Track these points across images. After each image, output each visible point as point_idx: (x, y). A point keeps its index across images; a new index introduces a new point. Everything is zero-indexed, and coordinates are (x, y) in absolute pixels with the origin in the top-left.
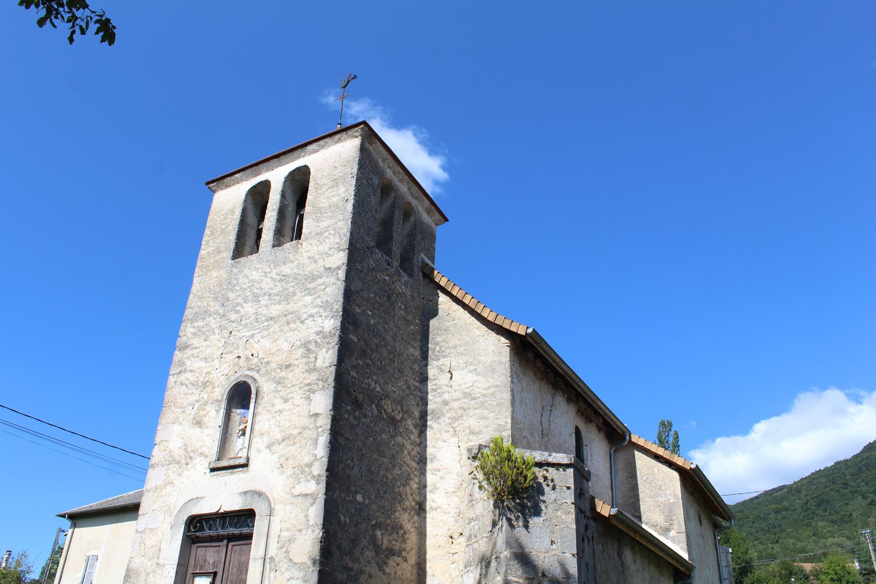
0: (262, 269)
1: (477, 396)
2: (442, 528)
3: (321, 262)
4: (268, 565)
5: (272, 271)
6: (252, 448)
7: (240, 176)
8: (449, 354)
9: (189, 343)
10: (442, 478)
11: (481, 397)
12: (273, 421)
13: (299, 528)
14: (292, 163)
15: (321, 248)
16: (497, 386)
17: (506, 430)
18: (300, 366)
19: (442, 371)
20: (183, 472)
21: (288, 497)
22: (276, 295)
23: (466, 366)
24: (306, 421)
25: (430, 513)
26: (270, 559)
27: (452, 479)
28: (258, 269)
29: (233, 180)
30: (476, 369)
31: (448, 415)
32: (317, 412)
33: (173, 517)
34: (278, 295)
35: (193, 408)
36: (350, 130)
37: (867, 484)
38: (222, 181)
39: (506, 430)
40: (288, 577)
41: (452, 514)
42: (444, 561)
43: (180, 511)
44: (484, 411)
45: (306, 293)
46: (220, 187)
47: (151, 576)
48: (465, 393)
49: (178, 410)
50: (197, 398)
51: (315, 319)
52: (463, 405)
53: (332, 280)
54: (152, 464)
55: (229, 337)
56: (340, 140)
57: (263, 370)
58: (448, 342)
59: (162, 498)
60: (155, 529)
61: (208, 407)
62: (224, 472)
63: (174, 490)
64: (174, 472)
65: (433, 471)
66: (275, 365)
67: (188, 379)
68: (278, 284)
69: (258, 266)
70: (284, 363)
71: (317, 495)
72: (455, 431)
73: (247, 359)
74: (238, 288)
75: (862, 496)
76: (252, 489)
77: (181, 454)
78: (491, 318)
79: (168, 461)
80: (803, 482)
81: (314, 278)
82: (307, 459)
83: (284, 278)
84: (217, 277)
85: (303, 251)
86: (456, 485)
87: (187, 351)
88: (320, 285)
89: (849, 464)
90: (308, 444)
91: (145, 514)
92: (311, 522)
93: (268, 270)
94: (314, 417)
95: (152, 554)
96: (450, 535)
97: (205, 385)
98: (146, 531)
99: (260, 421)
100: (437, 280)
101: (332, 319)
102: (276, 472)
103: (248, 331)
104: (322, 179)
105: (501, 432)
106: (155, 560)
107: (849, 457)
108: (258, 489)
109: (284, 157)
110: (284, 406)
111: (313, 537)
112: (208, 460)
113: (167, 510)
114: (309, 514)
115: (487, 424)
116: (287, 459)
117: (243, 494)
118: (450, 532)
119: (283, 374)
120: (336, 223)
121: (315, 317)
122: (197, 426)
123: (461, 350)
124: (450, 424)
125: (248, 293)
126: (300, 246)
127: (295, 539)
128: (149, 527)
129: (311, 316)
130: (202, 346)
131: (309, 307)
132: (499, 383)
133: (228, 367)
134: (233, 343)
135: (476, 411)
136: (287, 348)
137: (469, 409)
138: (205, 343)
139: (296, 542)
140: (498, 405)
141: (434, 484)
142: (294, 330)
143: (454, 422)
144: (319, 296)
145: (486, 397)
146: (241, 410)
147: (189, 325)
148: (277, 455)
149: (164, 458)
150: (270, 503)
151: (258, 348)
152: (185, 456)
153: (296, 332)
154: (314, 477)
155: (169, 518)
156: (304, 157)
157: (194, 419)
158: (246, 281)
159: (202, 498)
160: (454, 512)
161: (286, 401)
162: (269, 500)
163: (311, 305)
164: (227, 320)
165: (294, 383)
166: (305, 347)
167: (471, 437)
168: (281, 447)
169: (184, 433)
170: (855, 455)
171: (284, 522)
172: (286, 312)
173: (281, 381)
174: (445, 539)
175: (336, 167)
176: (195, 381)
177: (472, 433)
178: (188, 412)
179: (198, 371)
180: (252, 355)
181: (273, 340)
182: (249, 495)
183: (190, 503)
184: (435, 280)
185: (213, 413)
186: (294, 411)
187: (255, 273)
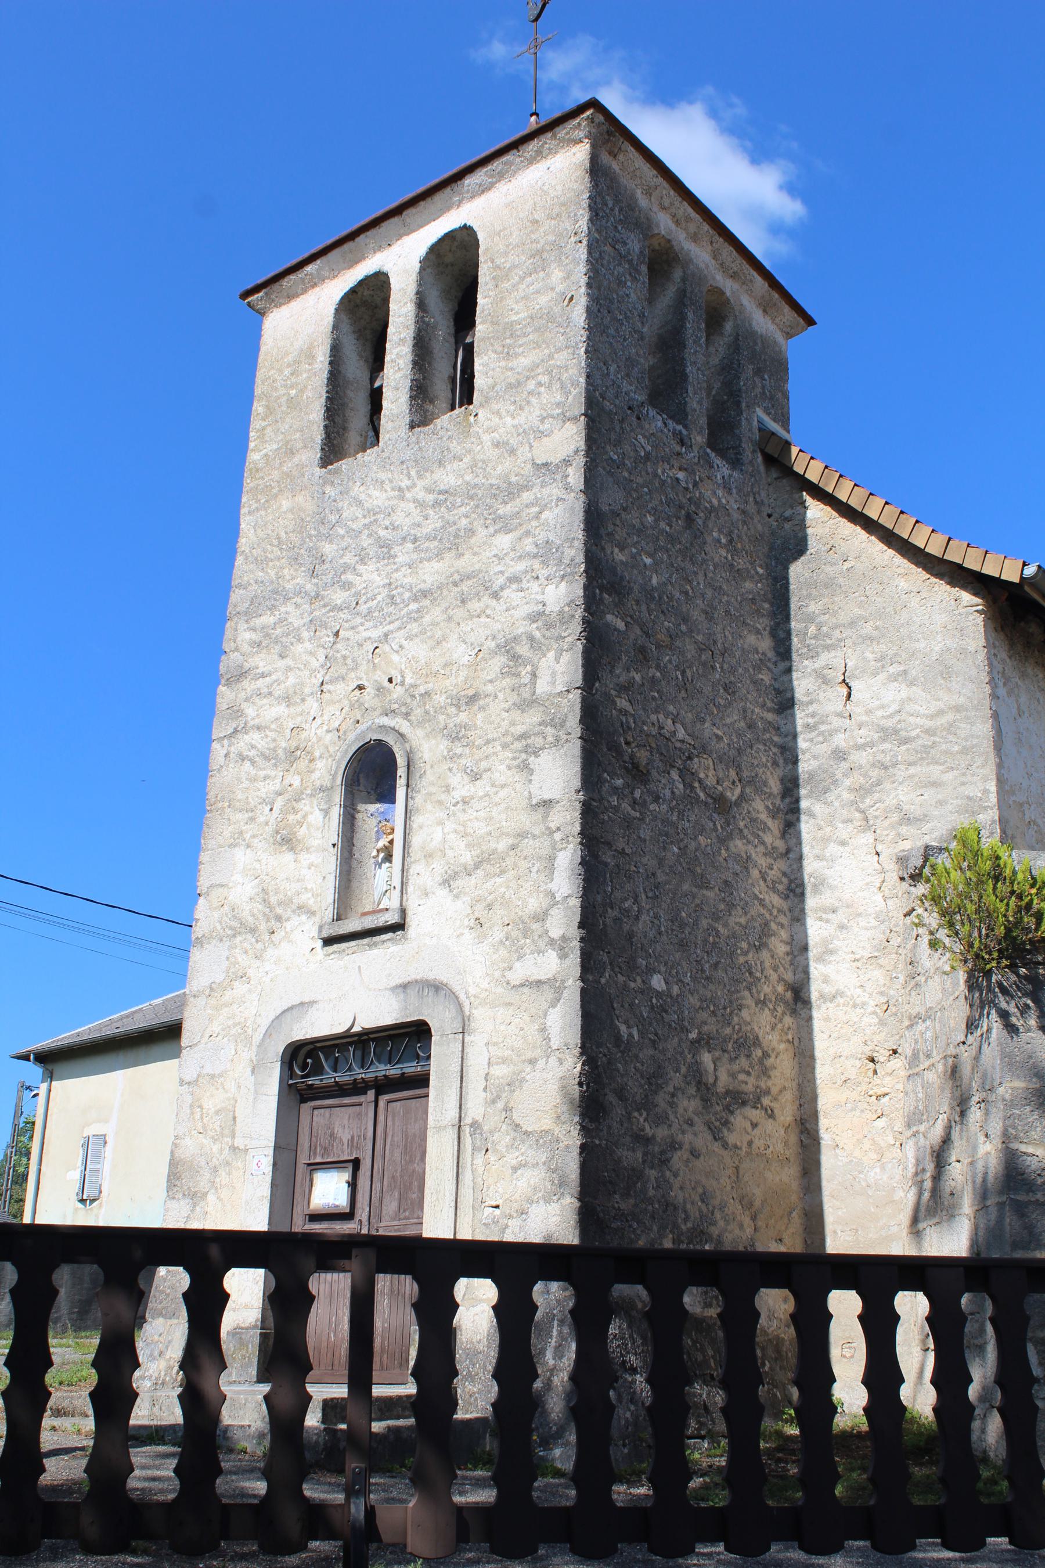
0: (391, 481)
1: (913, 734)
2: (849, 1040)
3: (524, 453)
4: (467, 1141)
5: (414, 485)
6: (410, 889)
8: (840, 640)
9: (247, 666)
10: (842, 927)
11: (922, 735)
12: (450, 826)
13: (529, 1055)
14: (433, 223)
15: (521, 419)
16: (957, 709)
17: (985, 808)
18: (501, 696)
19: (826, 681)
20: (264, 950)
21: (500, 990)
22: (429, 538)
23: (883, 667)
24: (525, 820)
25: (819, 1007)
26: (471, 1126)
27: (866, 929)
28: (383, 482)
29: (303, 280)
30: (905, 672)
31: (847, 782)
32: (546, 797)
33: (254, 1048)
34: (435, 538)
35: (271, 810)
36: (561, 127)
38: (276, 287)
39: (985, 808)
40: (514, 1162)
41: (870, 1009)
42: (857, 1113)
43: (268, 1034)
44: (931, 767)
45: (497, 527)
47: (222, 1173)
48: (882, 730)
49: (239, 816)
50: (278, 787)
51: (525, 585)
52: (880, 757)
53: (555, 491)
54: (197, 938)
55: (334, 643)
56: (539, 156)
57: (418, 712)
58: (835, 614)
59: (226, 1009)
60: (221, 1075)
61: (305, 806)
62: (353, 943)
63: (250, 991)
64: (246, 952)
65: (820, 914)
66: (444, 697)
67: (253, 747)
68: (431, 512)
69: (383, 476)
70: (462, 693)
71: (563, 982)
72: (866, 819)
73: (380, 689)
74: (341, 532)
76: (418, 977)
77: (255, 911)
78: (934, 548)
79: (231, 928)
81: (511, 491)
82: (534, 903)
83: (444, 497)
84: (291, 510)
85: (481, 431)
86: (876, 942)
87: (245, 683)
88: (527, 506)
90: (534, 869)
92: (555, 1043)
93: (405, 483)
94: (541, 810)
95: (218, 1129)
96: (869, 1054)
97: (292, 755)
98: (200, 1080)
99: (421, 827)
100: (799, 468)
101: (563, 584)
102: (468, 936)
103: (376, 626)
104: (506, 254)
105: (974, 813)
106: (226, 1139)
108: (430, 976)
110: (473, 789)
111: (561, 1074)
112: (317, 919)
113: (240, 1034)
114: (549, 1024)
115: (940, 797)
116: (489, 907)
117: (400, 990)
118: (870, 1048)
119: (463, 717)
120: (551, 357)
121: (524, 581)
122: (284, 848)
123: (868, 629)
124: (854, 803)
125: (365, 541)
126: (472, 419)
127: (523, 1080)
128: (205, 1071)
129: (515, 579)
131: (507, 560)
132: (962, 700)
133: (338, 713)
134: (345, 658)
135: (912, 770)
136: (467, 658)
137: (895, 764)
138: (281, 664)
139: (525, 1086)
140: (965, 751)
141: (826, 942)
142: (479, 616)
143: (863, 798)
144: (528, 533)
145: (934, 734)
146: (378, 806)
147: (243, 626)
148: (467, 899)
149: (220, 922)
150: (460, 1006)
151: (401, 663)
152: (265, 914)
153: (483, 619)
154: (552, 942)
155: (246, 1050)
156: (458, 206)
157: (277, 832)
158: (359, 513)
159: (312, 1003)
160: (872, 1003)
162: (457, 998)
163: (512, 555)
164: (325, 606)
165: (490, 736)
166: (508, 652)
167: (904, 830)
168: (473, 880)
169: (257, 866)
171: (495, 1044)
172: (456, 577)
173: (461, 734)
174: (858, 1063)
175: (537, 222)
176: (269, 749)
177: (907, 820)
178: (262, 819)
179: (273, 726)
180: (390, 680)
181: (431, 643)
182: (412, 992)
183: (288, 1015)
184: (795, 468)
185: (316, 817)
186: (497, 799)
187: (376, 493)
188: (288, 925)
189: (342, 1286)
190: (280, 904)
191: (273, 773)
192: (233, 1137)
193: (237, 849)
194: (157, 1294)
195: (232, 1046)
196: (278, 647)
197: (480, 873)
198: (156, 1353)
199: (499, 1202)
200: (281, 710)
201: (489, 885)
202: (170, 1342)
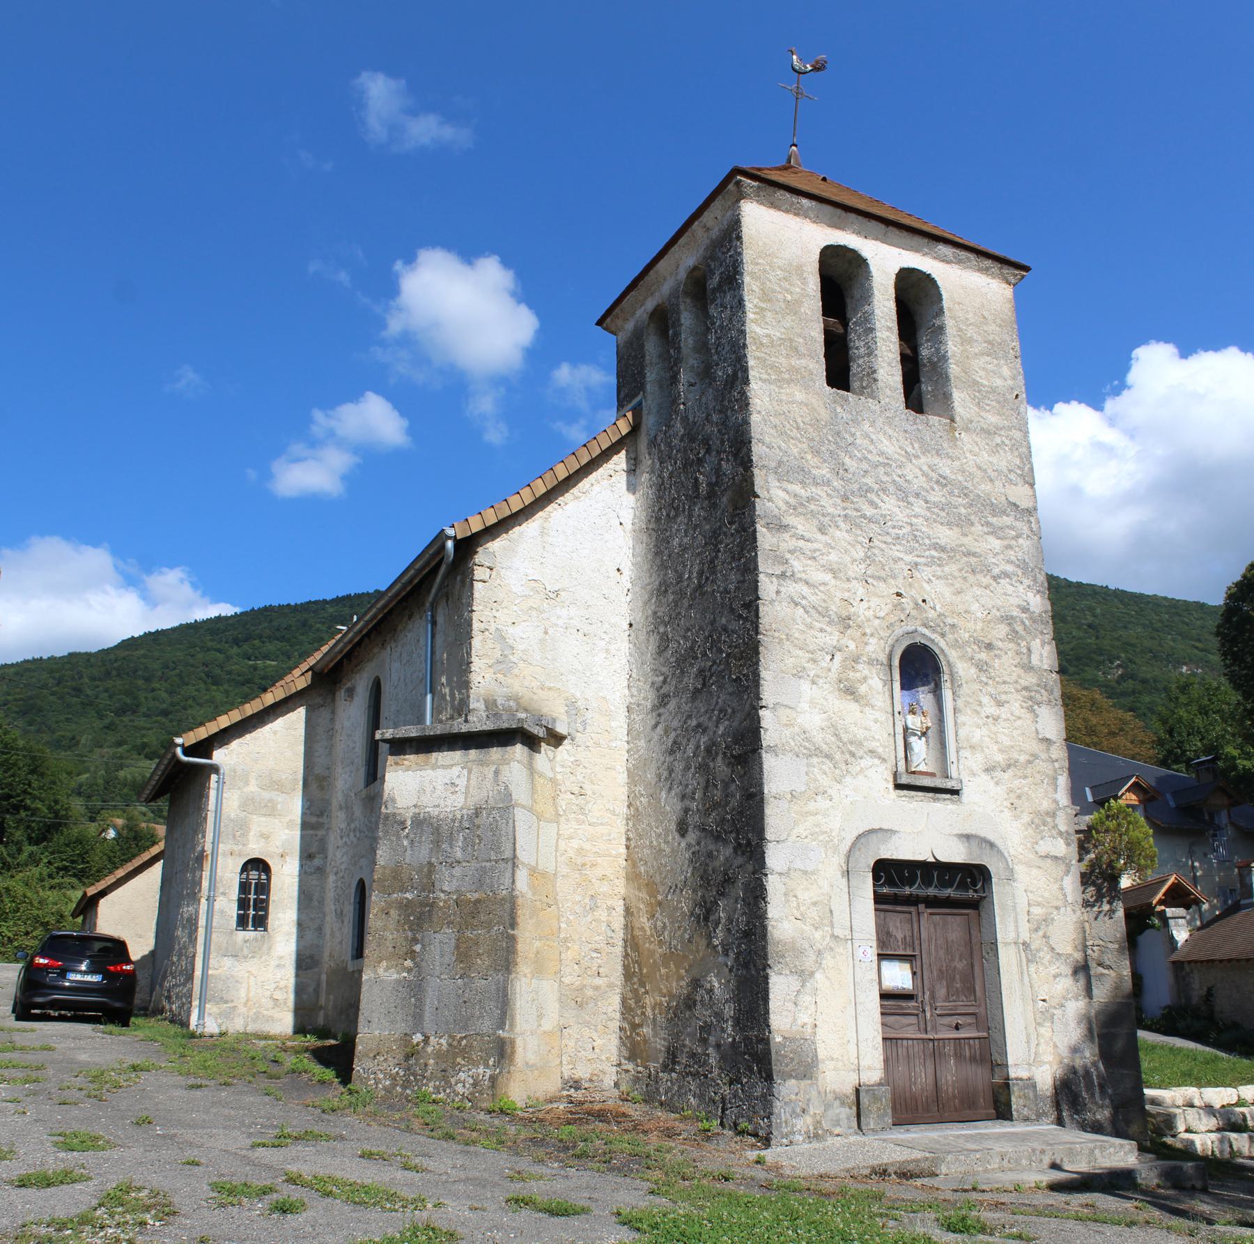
12: (985, 731)
15: (994, 460)
20: (844, 776)
22: (936, 505)
24: (1035, 747)
32: (1048, 736)
34: (943, 509)
37: (111, 697)
46: (759, 196)
47: (827, 955)
49: (800, 653)
56: (985, 271)
57: (950, 637)
60: (813, 873)
62: (920, 794)
64: (825, 773)
66: (967, 635)
67: (804, 598)
71: (1071, 861)
75: (97, 712)
80: (7, 670)
82: (1046, 805)
87: (786, 536)
89: (92, 660)
92: (1070, 899)
99: (964, 724)
102: (1007, 814)
107: (94, 650)
109: (894, 229)
111: (1075, 920)
117: (964, 839)
122: (849, 697)
130: (816, 541)
154: (1060, 834)
159: (893, 832)
161: (1000, 704)
164: (856, 510)
165: (1005, 679)
168: (1006, 776)
169: (825, 703)
170: (103, 650)
180: (924, 601)
182: (974, 843)
183: (874, 837)
188: (863, 763)
189: (916, 1050)
190: (851, 743)
193: (802, 681)
194: (780, 1058)
195: (823, 850)
197: (1010, 772)
198: (798, 1110)
199: (1047, 997)
200: (828, 577)
201: (1017, 782)
202: (809, 1100)
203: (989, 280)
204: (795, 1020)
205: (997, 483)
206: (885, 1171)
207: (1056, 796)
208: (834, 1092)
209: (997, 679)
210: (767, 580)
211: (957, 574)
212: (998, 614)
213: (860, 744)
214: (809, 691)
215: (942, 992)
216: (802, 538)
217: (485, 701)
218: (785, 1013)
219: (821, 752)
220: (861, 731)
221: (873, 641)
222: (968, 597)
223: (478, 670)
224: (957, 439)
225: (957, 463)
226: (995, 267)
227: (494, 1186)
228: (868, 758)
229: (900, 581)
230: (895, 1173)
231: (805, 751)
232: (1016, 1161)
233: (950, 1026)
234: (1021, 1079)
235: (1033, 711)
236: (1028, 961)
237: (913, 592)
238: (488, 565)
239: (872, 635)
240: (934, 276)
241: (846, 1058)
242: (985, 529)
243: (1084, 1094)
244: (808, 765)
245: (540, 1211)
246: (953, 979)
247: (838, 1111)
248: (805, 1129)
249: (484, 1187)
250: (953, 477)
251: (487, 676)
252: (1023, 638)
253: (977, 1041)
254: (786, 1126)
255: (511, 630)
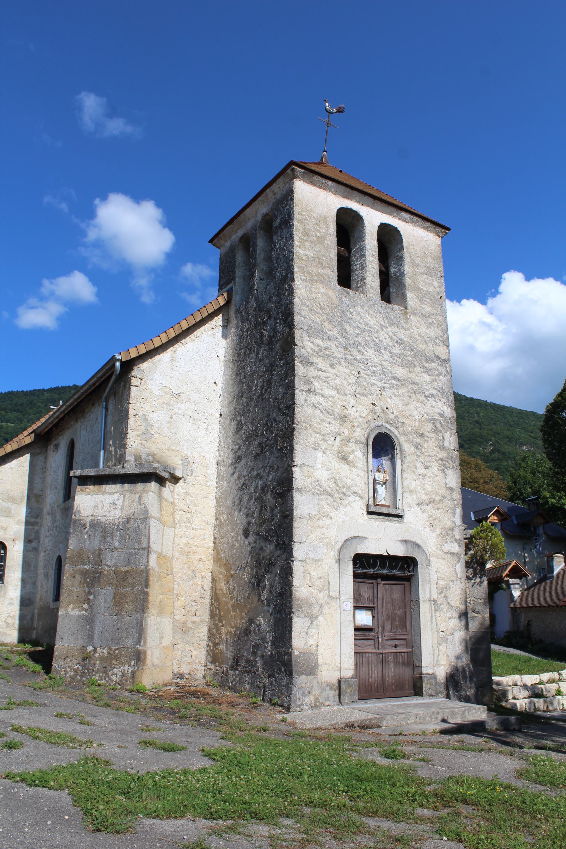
7: (331, 186)
12: (418, 483)
13: (451, 578)
20: (339, 506)
21: (440, 552)
24: (445, 492)
29: (323, 183)
32: (451, 486)
34: (399, 358)
38: (311, 174)
46: (304, 178)
49: (317, 435)
56: (426, 228)
57: (401, 429)
61: (352, 446)
62: (381, 517)
64: (329, 504)
66: (410, 428)
67: (321, 404)
79: (318, 490)
82: (449, 524)
87: (312, 368)
91: (303, 542)
92: (459, 576)
99: (407, 479)
102: (428, 529)
108: (414, 540)
109: (378, 202)
117: (404, 543)
122: (344, 462)
127: (450, 587)
130: (328, 372)
154: (456, 540)
159: (365, 538)
161: (426, 468)
164: (351, 355)
168: (428, 508)
169: (330, 465)
171: (439, 572)
180: (387, 408)
183: (354, 541)
188: (350, 499)
189: (373, 659)
190: (344, 488)
191: (333, 422)
192: (329, 590)
193: (317, 452)
194: (297, 664)
195: (325, 548)
196: (328, 361)
197: (430, 506)
198: (306, 692)
199: (444, 630)
200: (334, 393)
201: (434, 512)
202: (312, 687)
203: (428, 233)
204: (306, 643)
205: (429, 344)
206: (353, 725)
207: (454, 519)
208: (327, 682)
209: (426, 454)
210: (300, 393)
211: (406, 394)
212: (427, 417)
213: (349, 488)
214: (321, 458)
215: (388, 627)
216: (321, 370)
217: (135, 456)
218: (301, 639)
219: (327, 492)
220: (350, 481)
221: (358, 430)
222: (412, 407)
223: (131, 438)
224: (408, 319)
225: (408, 332)
226: (432, 227)
227: (132, 734)
228: (353, 497)
229: (375, 396)
230: (358, 726)
231: (318, 492)
232: (424, 718)
233: (392, 646)
234: (429, 674)
235: (444, 472)
236: (436, 610)
237: (381, 403)
238: (140, 377)
239: (358, 427)
240: (399, 229)
241: (333, 664)
242: (422, 370)
243: (462, 682)
244: (319, 500)
245: (159, 749)
246: (395, 620)
247: (328, 693)
248: (309, 702)
249: (127, 734)
250: (406, 340)
251: (136, 441)
252: (440, 431)
253: (406, 654)
254: (299, 701)
255: (151, 415)
